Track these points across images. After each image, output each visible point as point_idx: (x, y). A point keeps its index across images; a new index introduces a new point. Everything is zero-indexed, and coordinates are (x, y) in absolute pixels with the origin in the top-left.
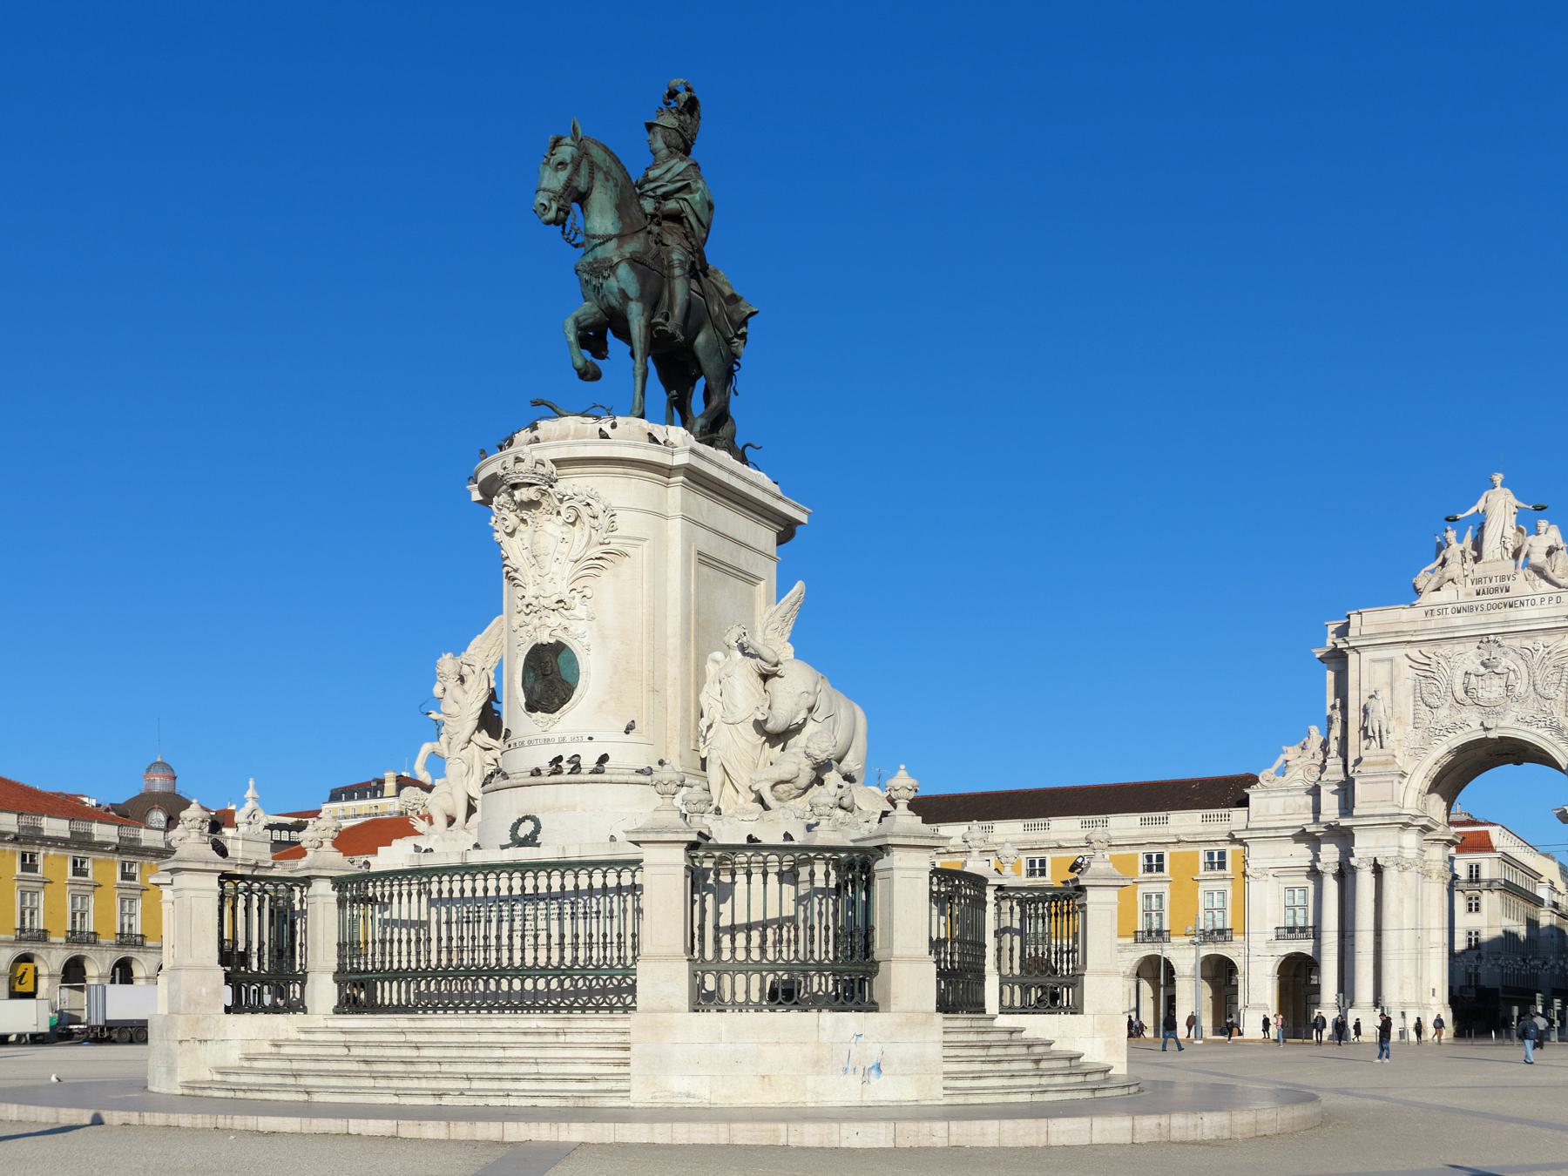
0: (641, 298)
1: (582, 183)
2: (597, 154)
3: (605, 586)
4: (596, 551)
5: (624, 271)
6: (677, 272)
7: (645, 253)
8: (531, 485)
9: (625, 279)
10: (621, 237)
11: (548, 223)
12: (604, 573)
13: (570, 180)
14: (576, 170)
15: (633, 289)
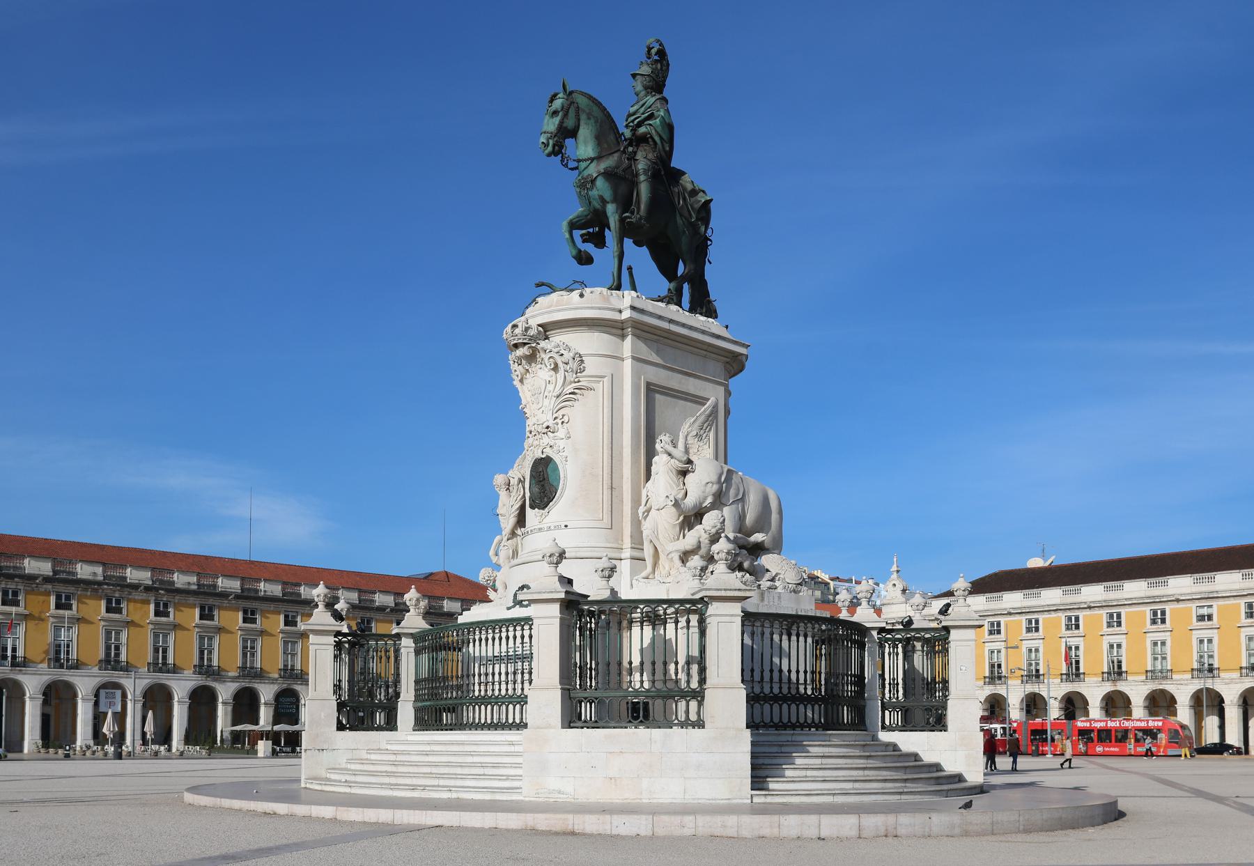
0: (615, 200)
1: (570, 123)
3: (578, 413)
4: (569, 389)
5: (600, 182)
6: (642, 178)
7: (617, 167)
8: (525, 344)
9: (602, 188)
11: (549, 155)
12: (576, 404)
13: (561, 122)
15: (608, 195)
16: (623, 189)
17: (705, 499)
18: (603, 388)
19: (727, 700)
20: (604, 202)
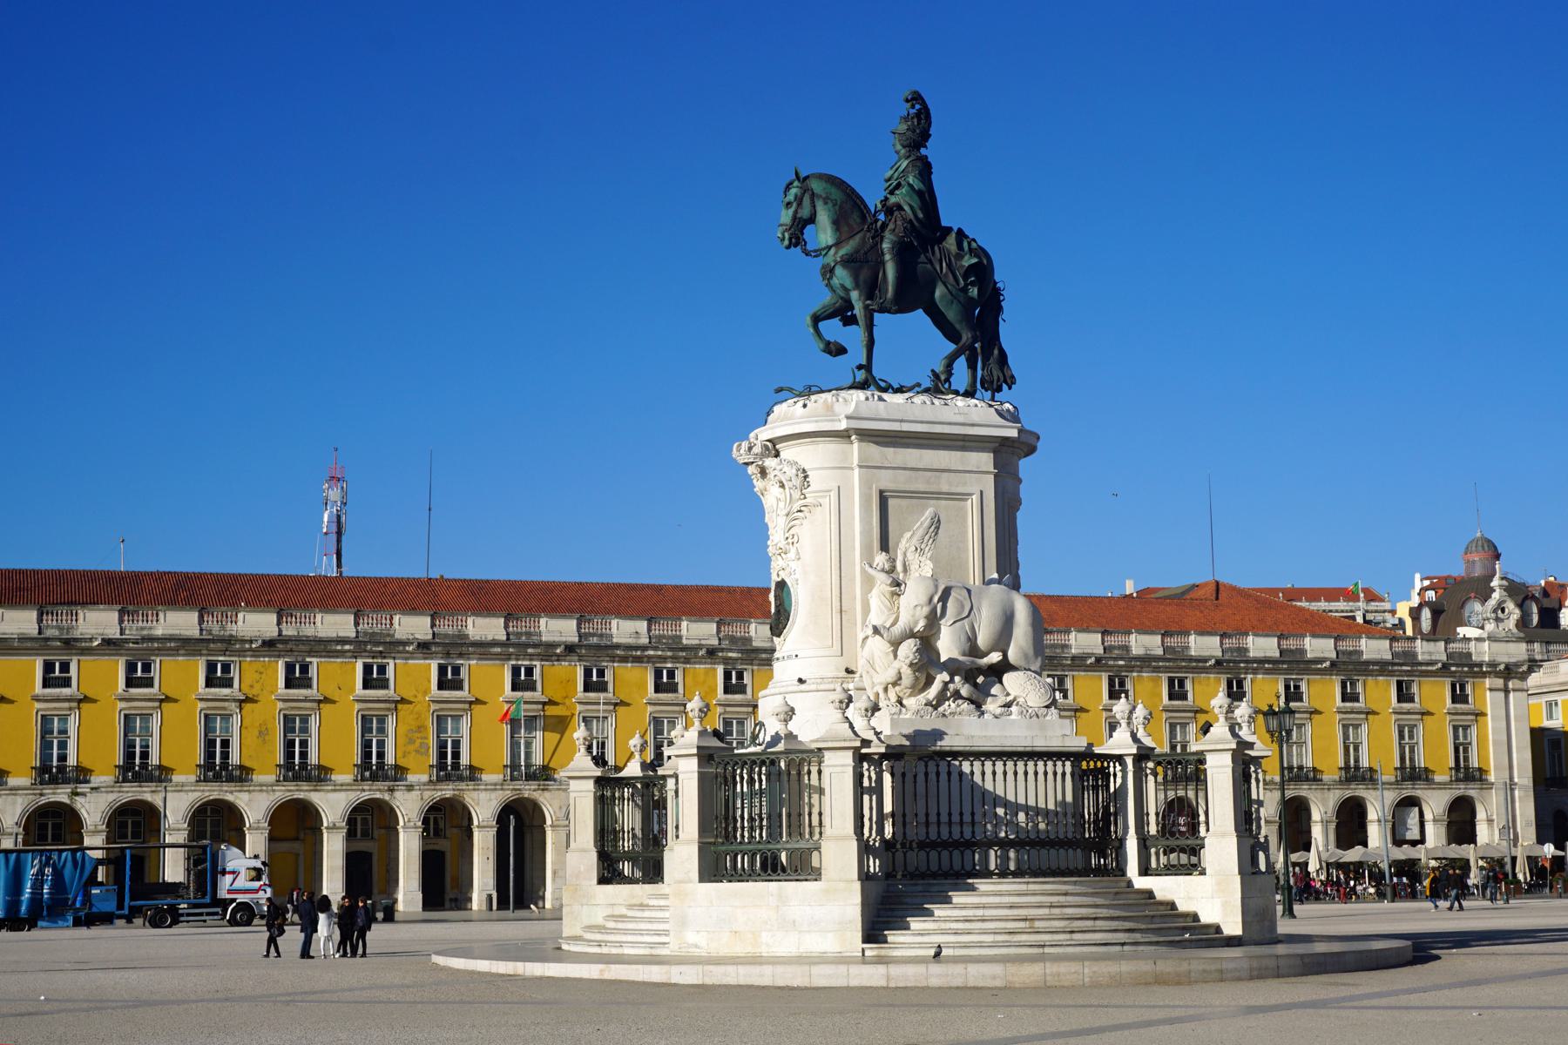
1: (805, 212)
2: (816, 186)
4: (796, 507)
6: (887, 257)
9: (842, 276)
10: (838, 244)
11: (788, 247)
13: (796, 212)
14: (800, 204)
15: (849, 283)
16: (865, 274)
17: (916, 623)
18: (829, 502)
19: (839, 854)
20: (847, 290)
